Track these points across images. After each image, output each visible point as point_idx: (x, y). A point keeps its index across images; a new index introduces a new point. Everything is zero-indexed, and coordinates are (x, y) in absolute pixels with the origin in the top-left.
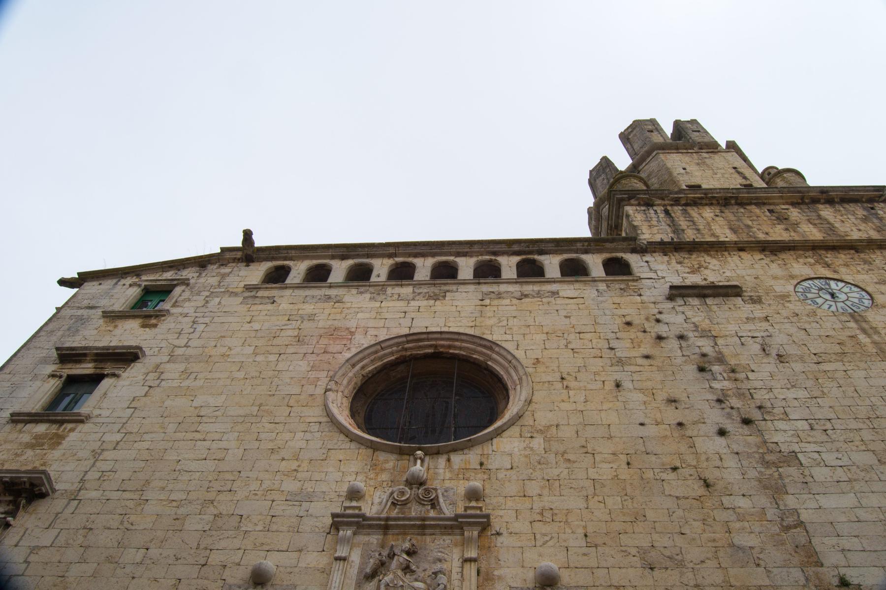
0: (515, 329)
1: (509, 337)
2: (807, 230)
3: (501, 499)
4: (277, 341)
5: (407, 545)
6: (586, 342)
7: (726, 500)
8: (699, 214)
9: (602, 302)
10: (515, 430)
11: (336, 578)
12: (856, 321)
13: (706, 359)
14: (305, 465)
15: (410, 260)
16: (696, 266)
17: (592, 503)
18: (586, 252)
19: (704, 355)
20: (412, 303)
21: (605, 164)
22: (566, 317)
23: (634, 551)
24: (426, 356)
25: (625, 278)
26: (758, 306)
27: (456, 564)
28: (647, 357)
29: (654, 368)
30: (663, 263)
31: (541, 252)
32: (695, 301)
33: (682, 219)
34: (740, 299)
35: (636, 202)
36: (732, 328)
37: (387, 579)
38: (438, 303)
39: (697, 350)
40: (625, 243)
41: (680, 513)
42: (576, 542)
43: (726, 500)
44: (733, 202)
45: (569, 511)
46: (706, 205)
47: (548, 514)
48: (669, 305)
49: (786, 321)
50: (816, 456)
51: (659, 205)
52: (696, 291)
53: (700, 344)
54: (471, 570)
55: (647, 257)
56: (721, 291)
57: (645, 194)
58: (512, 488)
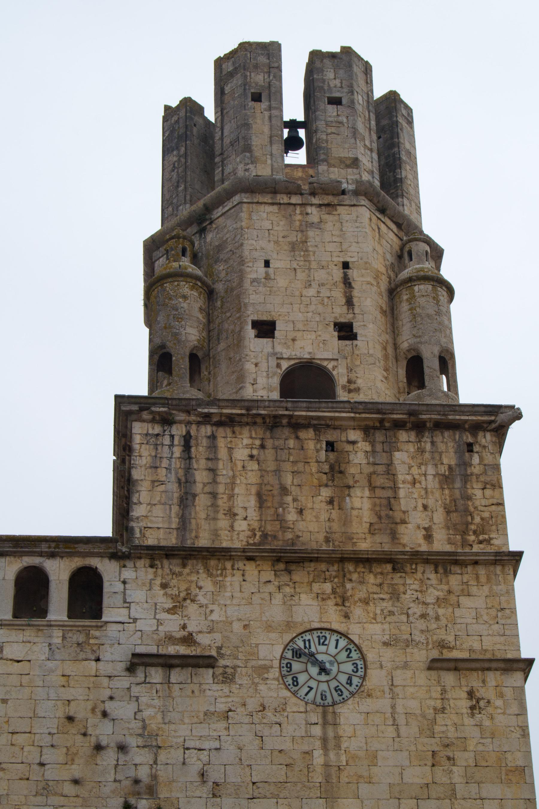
2: (357, 503)
6: (17, 749)
8: (230, 449)
9: (52, 671)
12: (325, 723)
13: (137, 788)
16: (182, 595)
18: (52, 555)
19: (137, 782)
21: (190, 107)
25: (87, 622)
26: (226, 689)
28: (76, 782)
29: (79, 801)
30: (144, 584)
32: (156, 675)
33: (203, 463)
34: (211, 671)
35: (150, 417)
36: (183, 731)
39: (132, 773)
40: (102, 546)
44: (285, 421)
46: (247, 424)
48: (124, 682)
49: (247, 720)
51: (180, 422)
52: (161, 661)
53: (137, 760)
55: (128, 574)
56: (190, 661)
57: (163, 405)
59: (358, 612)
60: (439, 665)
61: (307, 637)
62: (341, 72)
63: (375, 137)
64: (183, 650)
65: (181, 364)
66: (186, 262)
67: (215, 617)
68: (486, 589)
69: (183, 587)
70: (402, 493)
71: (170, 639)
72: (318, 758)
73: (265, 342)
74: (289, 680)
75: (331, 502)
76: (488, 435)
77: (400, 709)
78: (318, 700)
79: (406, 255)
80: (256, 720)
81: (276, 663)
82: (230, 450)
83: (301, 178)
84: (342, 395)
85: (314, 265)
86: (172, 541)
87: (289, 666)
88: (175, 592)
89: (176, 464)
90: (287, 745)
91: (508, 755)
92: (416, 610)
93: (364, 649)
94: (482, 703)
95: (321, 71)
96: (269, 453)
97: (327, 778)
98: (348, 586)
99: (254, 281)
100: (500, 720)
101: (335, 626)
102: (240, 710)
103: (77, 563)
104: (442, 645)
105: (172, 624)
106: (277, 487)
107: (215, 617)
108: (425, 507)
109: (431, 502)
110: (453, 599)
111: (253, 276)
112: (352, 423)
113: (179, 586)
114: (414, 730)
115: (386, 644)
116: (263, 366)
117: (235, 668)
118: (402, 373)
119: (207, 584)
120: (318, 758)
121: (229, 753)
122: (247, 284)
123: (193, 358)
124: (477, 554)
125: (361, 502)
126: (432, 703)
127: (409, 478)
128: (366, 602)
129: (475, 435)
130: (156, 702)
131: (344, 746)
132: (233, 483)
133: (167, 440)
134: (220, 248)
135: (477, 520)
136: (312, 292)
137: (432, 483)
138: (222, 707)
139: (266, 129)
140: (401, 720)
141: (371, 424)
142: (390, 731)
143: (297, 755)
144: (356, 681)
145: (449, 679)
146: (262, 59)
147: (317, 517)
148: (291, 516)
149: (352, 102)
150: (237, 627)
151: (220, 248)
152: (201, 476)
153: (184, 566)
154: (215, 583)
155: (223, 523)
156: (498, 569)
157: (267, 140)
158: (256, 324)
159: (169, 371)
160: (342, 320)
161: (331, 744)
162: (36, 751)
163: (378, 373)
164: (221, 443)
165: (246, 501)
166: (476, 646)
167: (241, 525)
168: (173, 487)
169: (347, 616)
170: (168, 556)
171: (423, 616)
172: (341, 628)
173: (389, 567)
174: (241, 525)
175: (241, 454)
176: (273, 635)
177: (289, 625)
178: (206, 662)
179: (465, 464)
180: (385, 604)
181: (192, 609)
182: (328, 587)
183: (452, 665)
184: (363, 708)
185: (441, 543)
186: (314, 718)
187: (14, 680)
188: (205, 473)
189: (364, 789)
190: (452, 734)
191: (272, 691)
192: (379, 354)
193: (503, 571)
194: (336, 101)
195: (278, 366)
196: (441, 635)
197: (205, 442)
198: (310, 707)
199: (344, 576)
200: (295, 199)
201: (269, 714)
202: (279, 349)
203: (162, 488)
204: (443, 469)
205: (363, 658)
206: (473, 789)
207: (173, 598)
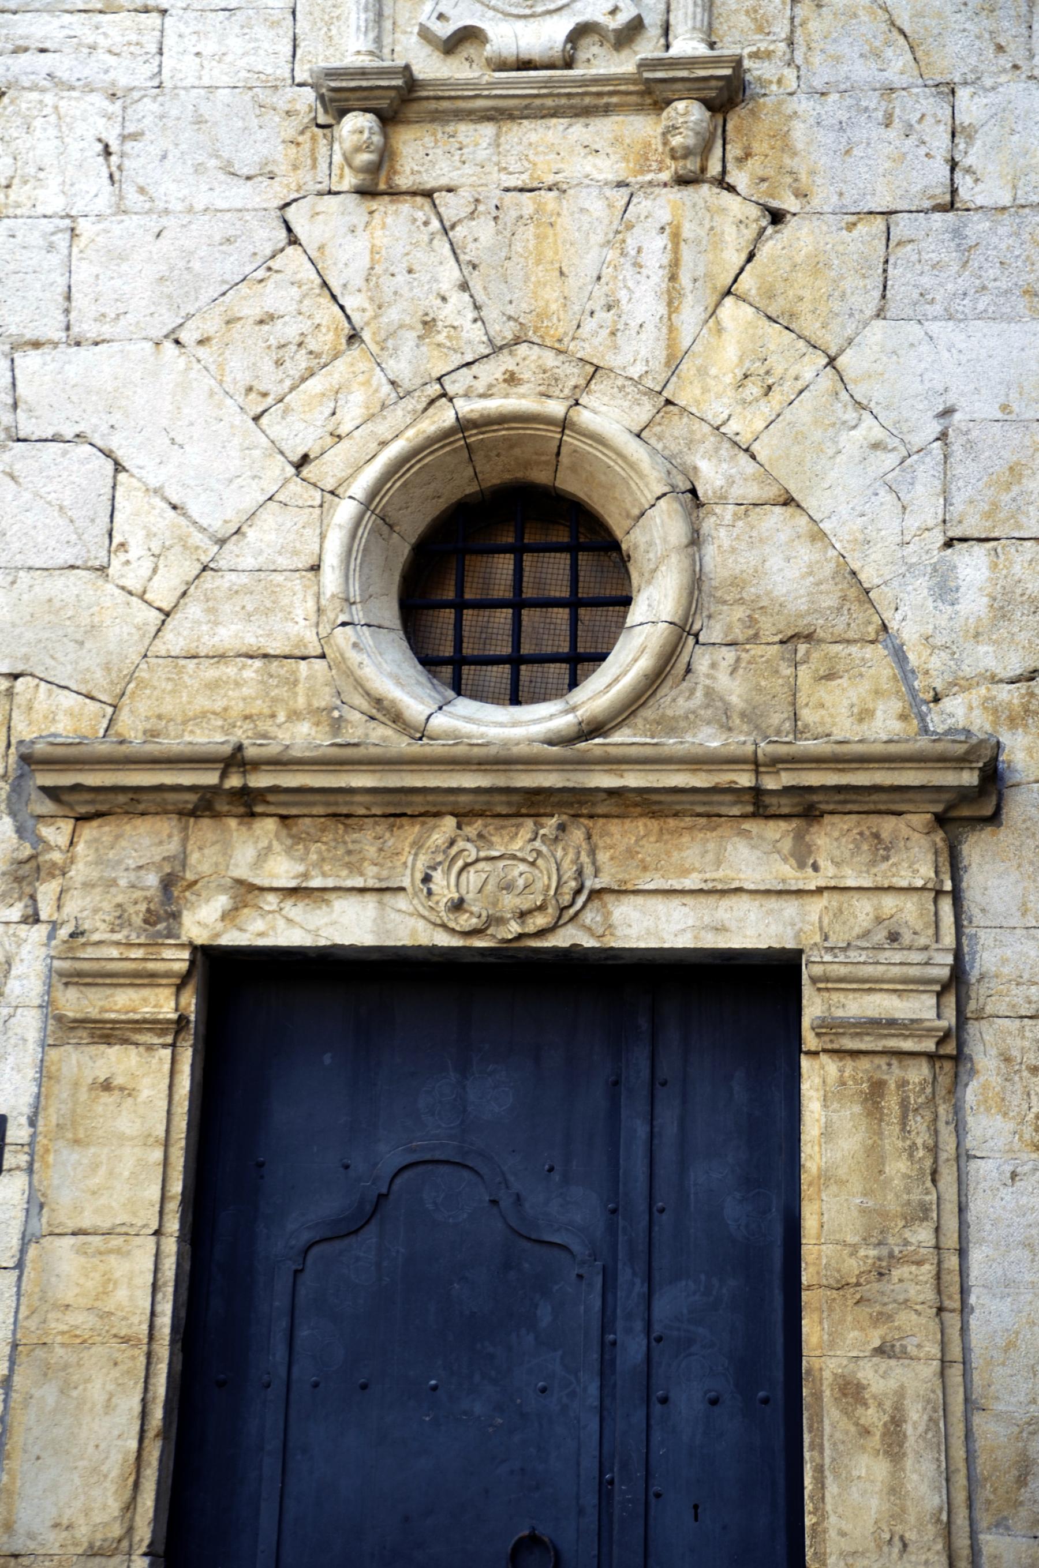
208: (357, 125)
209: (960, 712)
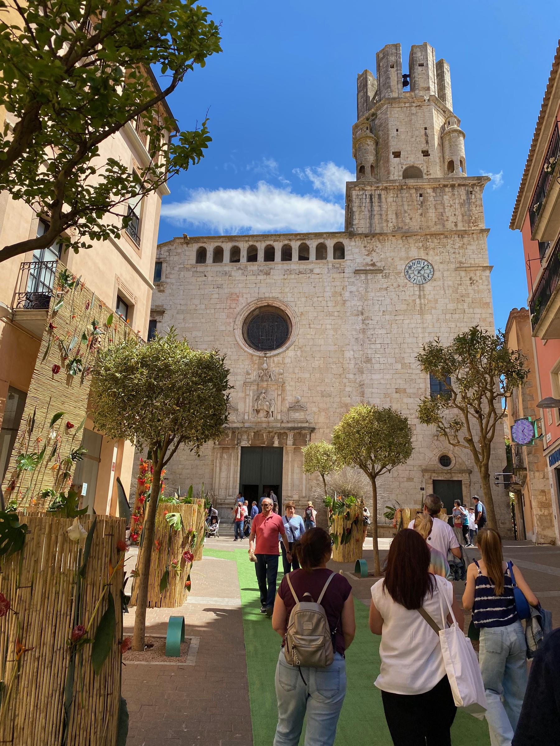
0: (296, 294)
1: (293, 300)
2: (431, 215)
3: (288, 374)
4: (212, 302)
5: (264, 391)
7: (347, 375)
8: (386, 198)
10: (293, 347)
11: (247, 400)
12: (420, 290)
14: (233, 362)
15: (255, 244)
17: (312, 376)
20: (259, 277)
22: (314, 287)
23: (320, 392)
24: (265, 306)
27: (276, 395)
31: (308, 239)
32: (363, 277)
33: (377, 204)
37: (260, 402)
38: (268, 276)
41: (334, 379)
42: (306, 389)
43: (347, 375)
45: (305, 378)
47: (300, 379)
49: (393, 290)
50: (378, 359)
54: (280, 398)
58: (291, 370)
59: (431, 252)
60: (459, 269)
61: (413, 261)
62: (423, 53)
63: (436, 78)
64: (371, 268)
65: (368, 170)
66: (368, 131)
67: (382, 256)
68: (477, 242)
69: (371, 247)
70: (446, 210)
71: (367, 264)
72: (418, 301)
73: (397, 159)
74: (408, 277)
75: (421, 215)
76: (478, 187)
77: (446, 285)
78: (418, 283)
79: (447, 123)
80: (396, 290)
81: (403, 271)
82: (386, 198)
83: (409, 97)
84: (425, 177)
85: (414, 129)
86: (367, 231)
87: (407, 272)
88: (369, 248)
89: (368, 205)
90: (407, 298)
91: (484, 299)
92: (452, 251)
93: (433, 265)
94: (475, 282)
95: (415, 53)
96: (400, 199)
97: (421, 308)
98: (428, 244)
99: (392, 137)
100: (481, 287)
101: (423, 258)
102: (391, 287)
103: (335, 241)
104: (461, 263)
105: (368, 260)
106: (403, 210)
107: (382, 256)
108: (455, 215)
109: (457, 213)
110: (465, 246)
111: (393, 135)
112: (429, 186)
113: (370, 247)
114: (451, 291)
115: (441, 263)
116: (397, 168)
117: (389, 273)
118: (446, 167)
119: (379, 246)
120: (418, 301)
121: (388, 301)
122: (390, 138)
123: (372, 166)
124: (474, 230)
125: (432, 214)
126: (457, 282)
127: (449, 205)
128: (434, 249)
129: (473, 188)
130: (364, 286)
131: (426, 297)
132: (387, 210)
133: (364, 197)
134: (380, 126)
135: (474, 218)
136: (413, 139)
137: (457, 206)
138: (385, 286)
139: (396, 79)
140: (446, 288)
141: (435, 186)
142: (442, 292)
143: (410, 301)
144: (430, 276)
145: (463, 274)
146: (394, 51)
147: (417, 220)
148: (408, 221)
149: (428, 64)
150: (390, 259)
151: (380, 126)
152: (376, 208)
153: (371, 240)
154: (382, 245)
155: (385, 224)
156: (481, 235)
157: (396, 83)
158: (393, 153)
159: (364, 173)
160: (424, 149)
161: (422, 297)
162: (325, 302)
163: (438, 168)
164: (383, 196)
165: (392, 216)
166: (473, 262)
167: (390, 225)
168: (367, 213)
169: (427, 254)
170: (366, 237)
171: (454, 253)
172: (426, 258)
173: (442, 236)
174: (390, 225)
175: (390, 200)
176: (402, 262)
177: (407, 258)
178: (380, 271)
179: (469, 199)
180: (440, 249)
181: (374, 254)
182: (421, 244)
183: (464, 269)
184: (433, 285)
185: (460, 227)
186: (416, 289)
187: (317, 280)
188: (378, 207)
189: (433, 311)
190: (464, 292)
191: (402, 280)
192: (438, 161)
193: (483, 236)
194: (421, 65)
195: (402, 167)
196: (460, 259)
197: (377, 196)
198: (415, 285)
199: (427, 240)
200: (407, 105)
201: (401, 288)
202: (402, 161)
203: (363, 213)
204: (461, 201)
205: (433, 268)
206: (471, 310)
207: (368, 251)
208: (436, 437)
209: (469, 468)
